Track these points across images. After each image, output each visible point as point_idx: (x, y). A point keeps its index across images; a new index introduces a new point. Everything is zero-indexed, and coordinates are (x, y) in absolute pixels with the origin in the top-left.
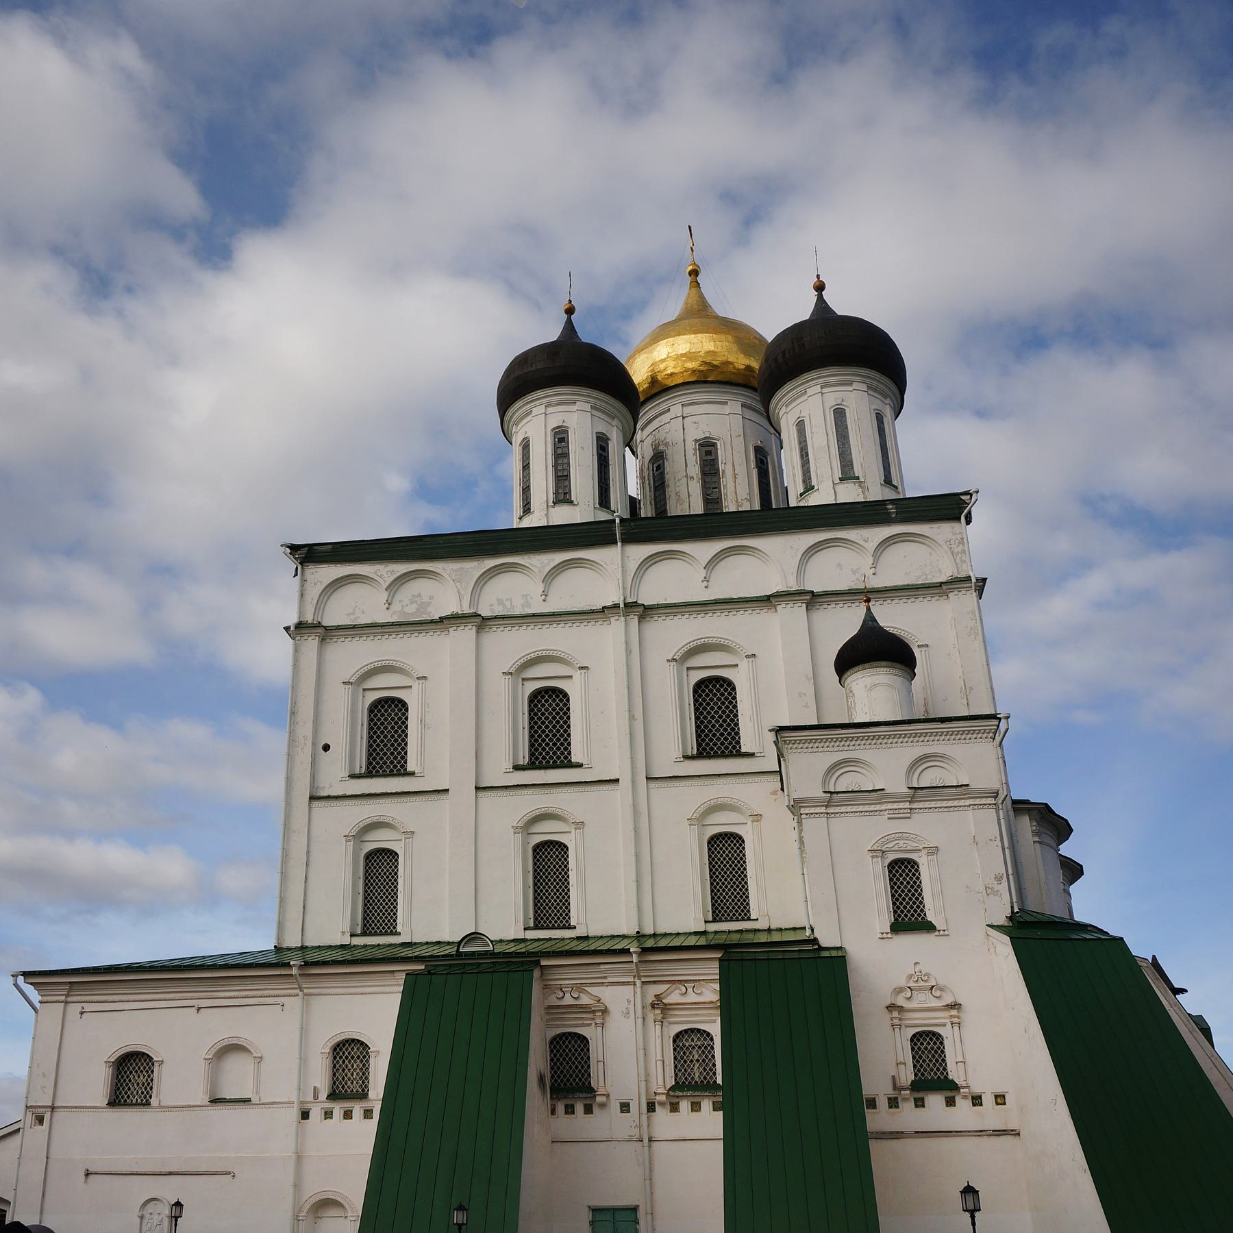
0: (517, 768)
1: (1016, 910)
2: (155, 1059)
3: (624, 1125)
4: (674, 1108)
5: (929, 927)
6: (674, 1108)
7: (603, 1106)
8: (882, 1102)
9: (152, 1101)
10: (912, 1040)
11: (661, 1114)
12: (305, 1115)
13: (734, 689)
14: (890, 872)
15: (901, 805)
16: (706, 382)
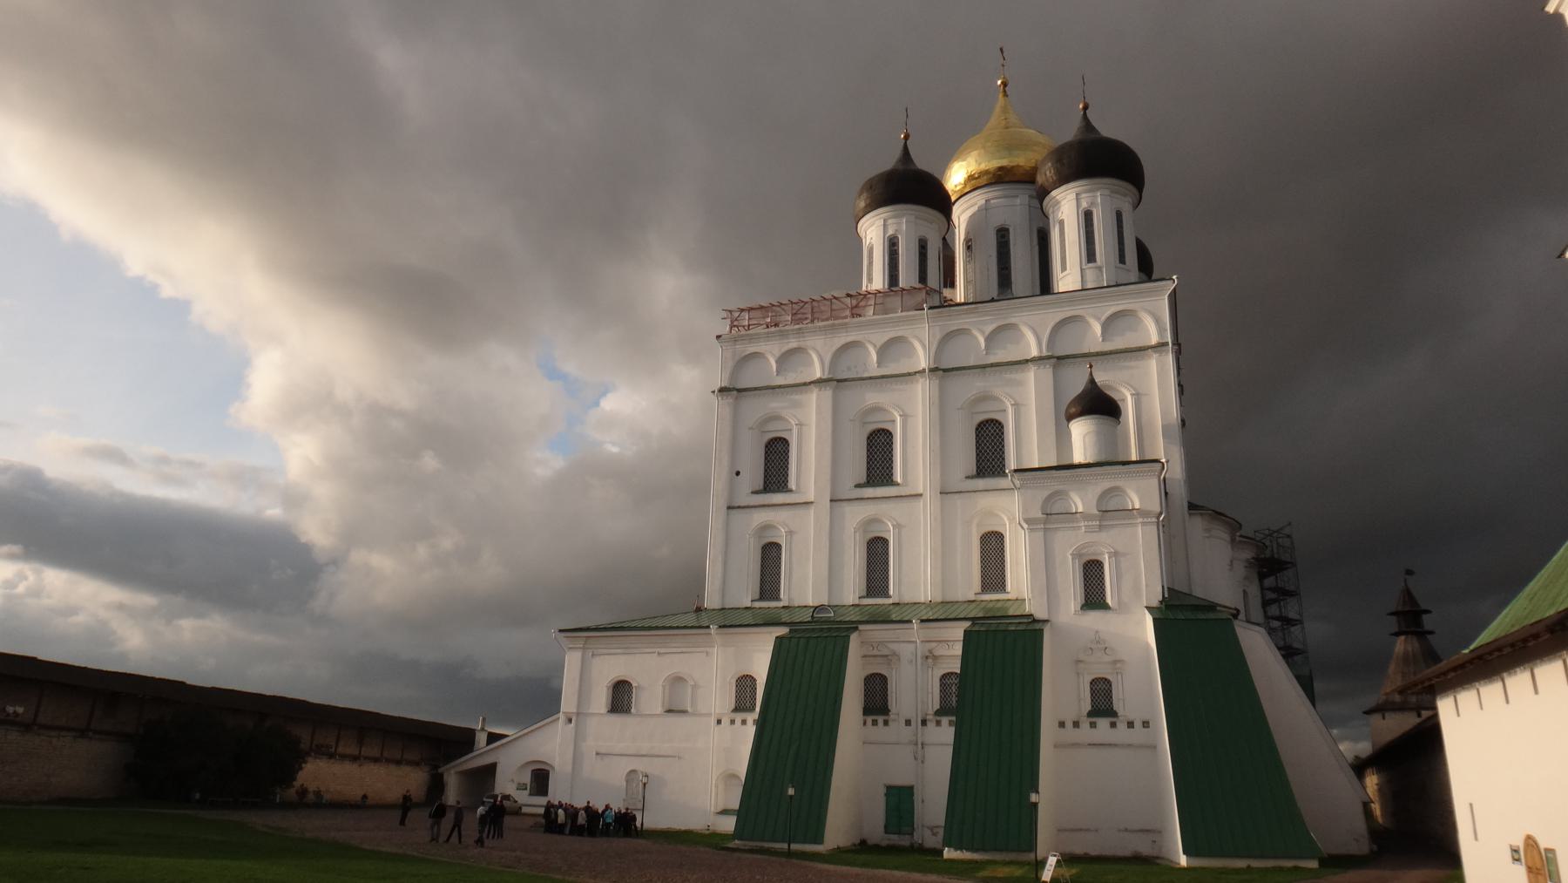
0: (858, 486)
1: (1166, 596)
2: (634, 685)
3: (907, 733)
4: (938, 723)
5: (1105, 607)
6: (938, 723)
7: (894, 720)
8: (1069, 724)
9: (632, 710)
10: (1091, 683)
11: (931, 726)
12: (719, 722)
13: (1003, 427)
14: (1084, 568)
15: (1094, 523)
16: (1003, 183)
